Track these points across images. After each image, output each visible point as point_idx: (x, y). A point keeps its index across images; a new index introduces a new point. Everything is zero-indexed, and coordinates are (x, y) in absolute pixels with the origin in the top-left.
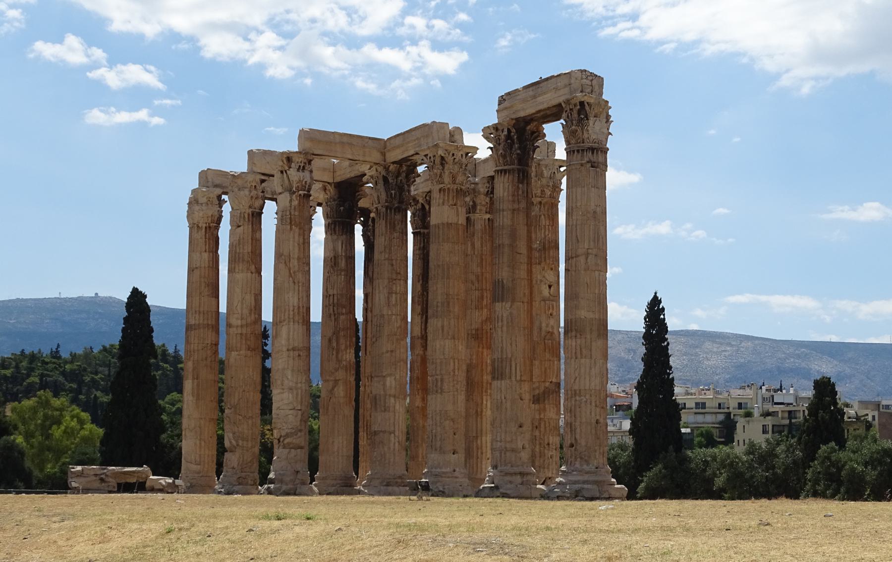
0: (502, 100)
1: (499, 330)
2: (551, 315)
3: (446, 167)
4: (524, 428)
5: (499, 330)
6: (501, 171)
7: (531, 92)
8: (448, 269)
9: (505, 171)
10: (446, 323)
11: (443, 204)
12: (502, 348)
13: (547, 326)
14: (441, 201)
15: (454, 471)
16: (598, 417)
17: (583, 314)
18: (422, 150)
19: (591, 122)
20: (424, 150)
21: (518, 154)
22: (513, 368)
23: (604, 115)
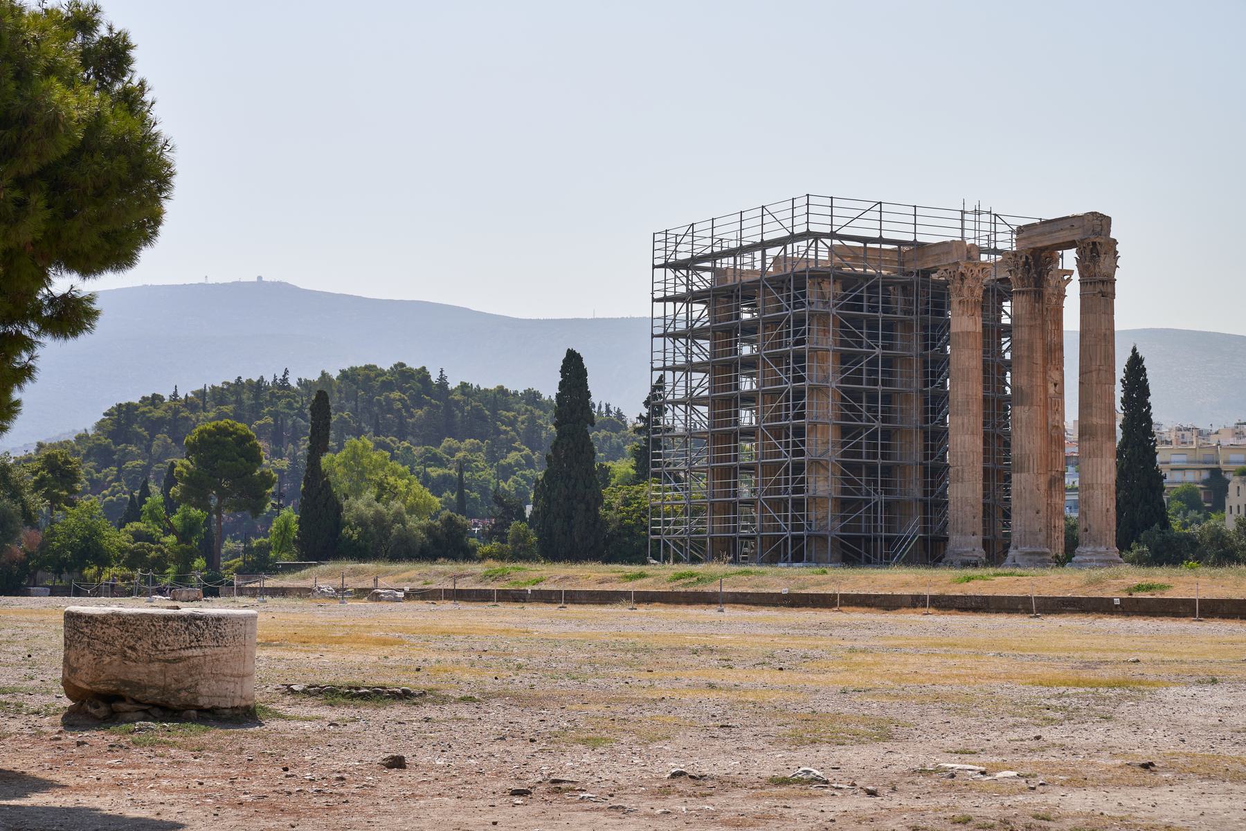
0: (1020, 230)
1: (1019, 432)
2: (1057, 410)
3: (966, 281)
4: (1041, 514)
5: (1019, 430)
6: (1020, 292)
7: (1047, 228)
8: (968, 372)
9: (1023, 293)
10: (966, 421)
11: (963, 314)
12: (1021, 446)
13: (1053, 421)
14: (961, 312)
15: (974, 550)
16: (1108, 507)
17: (1096, 420)
18: (942, 266)
19: (1102, 259)
20: (944, 265)
21: (1034, 277)
22: (1031, 462)
23: (1112, 253)
